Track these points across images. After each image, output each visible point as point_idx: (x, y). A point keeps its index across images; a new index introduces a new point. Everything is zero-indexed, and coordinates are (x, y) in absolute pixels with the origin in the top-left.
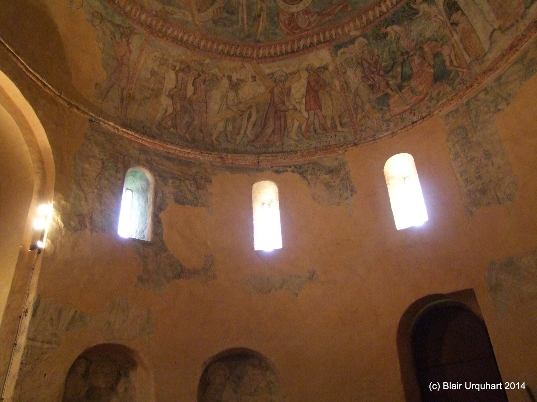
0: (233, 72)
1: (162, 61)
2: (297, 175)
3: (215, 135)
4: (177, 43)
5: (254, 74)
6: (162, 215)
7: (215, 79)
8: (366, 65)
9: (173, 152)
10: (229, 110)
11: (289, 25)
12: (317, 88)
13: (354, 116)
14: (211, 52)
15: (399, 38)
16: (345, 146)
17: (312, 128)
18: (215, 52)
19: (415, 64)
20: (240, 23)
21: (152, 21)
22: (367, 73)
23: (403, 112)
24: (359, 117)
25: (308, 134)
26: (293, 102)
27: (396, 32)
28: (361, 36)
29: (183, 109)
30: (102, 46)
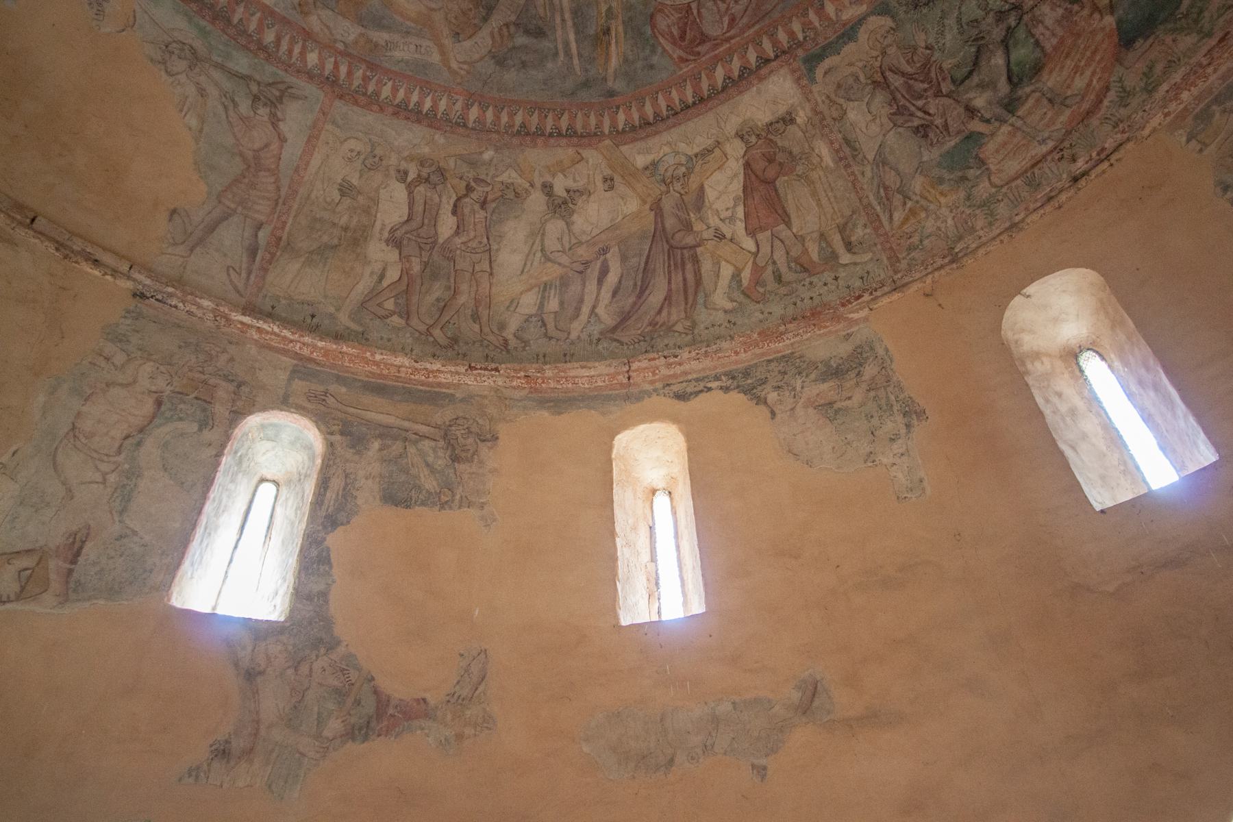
0: (554, 176)
1: (369, 161)
2: (737, 397)
3: (513, 325)
4: (407, 118)
5: (608, 172)
6: (335, 540)
7: (511, 195)
8: (896, 81)
9: (393, 370)
10: (549, 264)
11: (682, 38)
12: (771, 173)
13: (884, 219)
14: (498, 132)
16: (866, 297)
17: (768, 274)
18: (506, 132)
22: (903, 102)
23: (1033, 166)
24: (898, 216)
25: (762, 290)
26: (714, 221)
28: (872, 13)
29: (428, 270)
30: (194, 123)
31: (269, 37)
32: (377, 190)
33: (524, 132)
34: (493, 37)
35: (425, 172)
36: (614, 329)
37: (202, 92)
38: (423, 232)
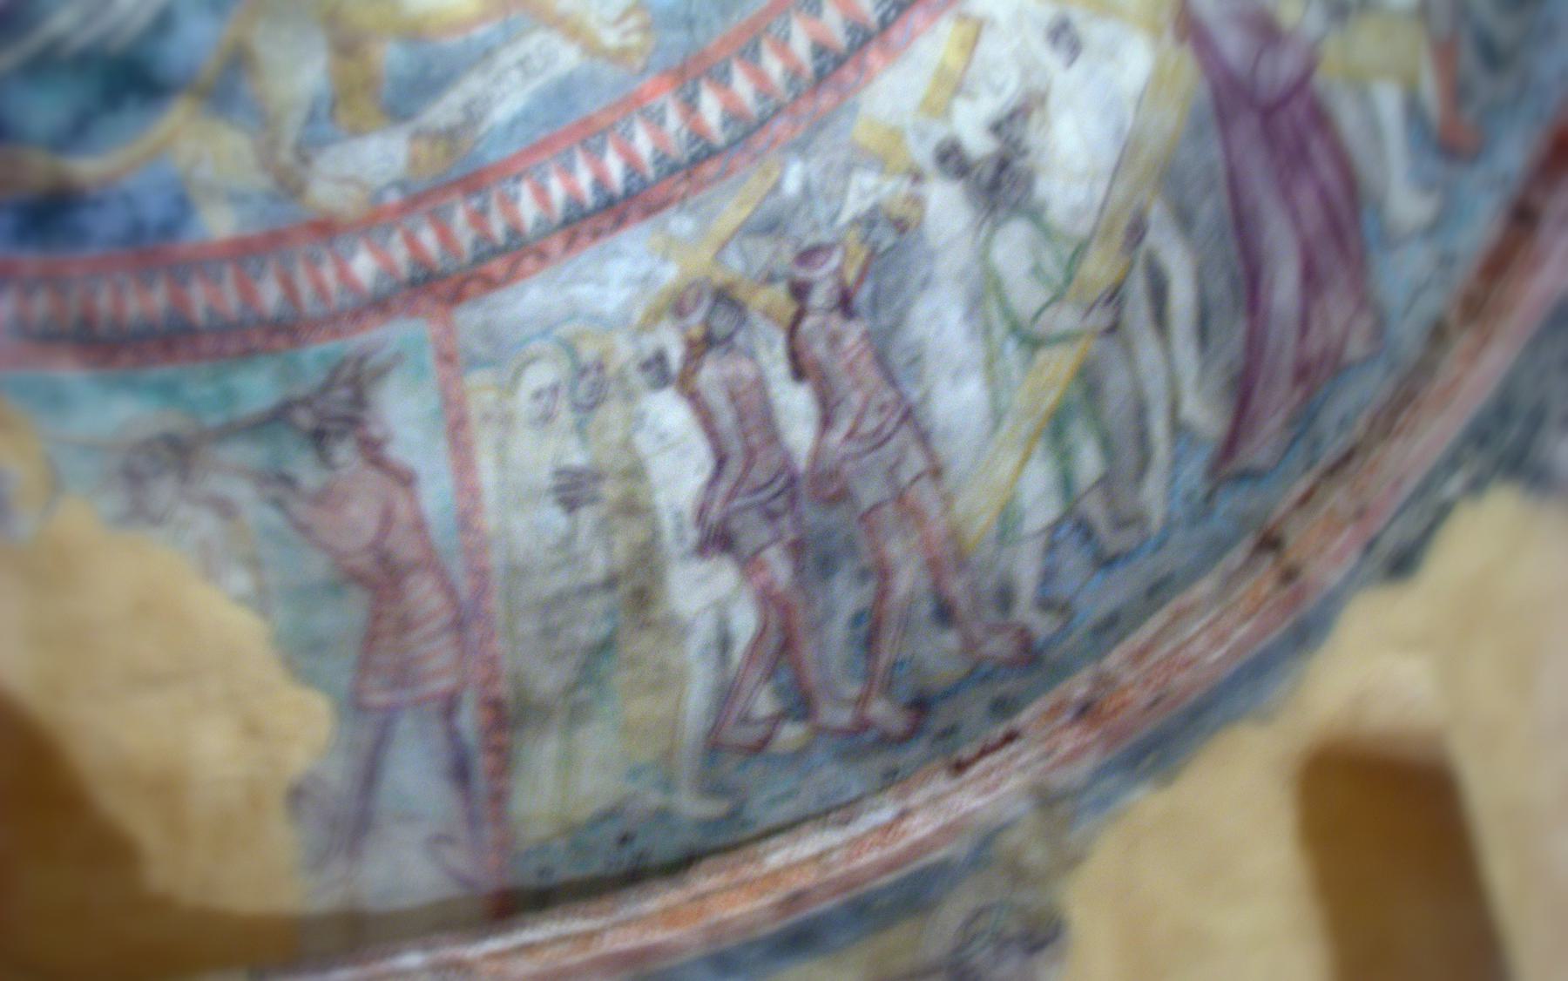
4: (596, 235)
7: (888, 239)
10: (1042, 356)
21: (411, 241)
31: (270, 295)
32: (627, 445)
35: (695, 321)
36: (1231, 445)
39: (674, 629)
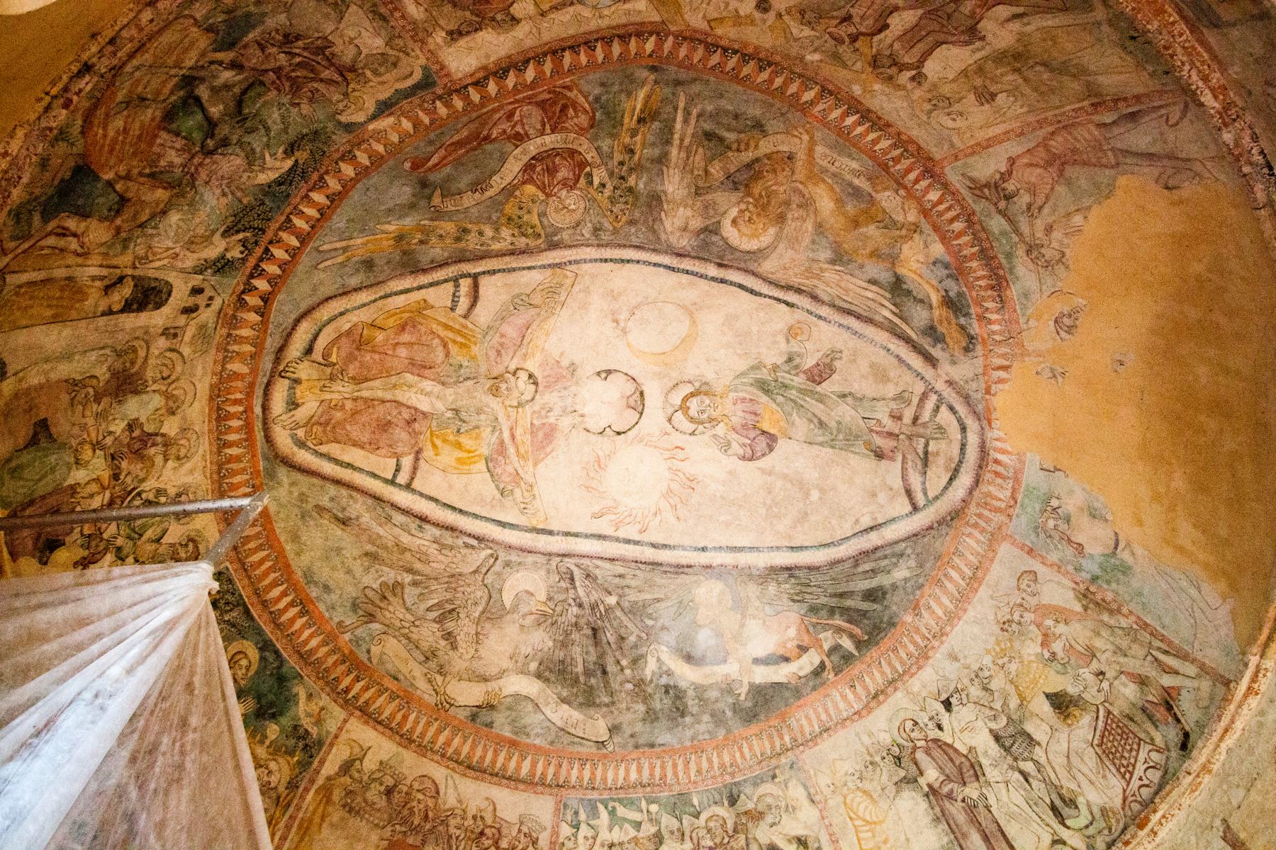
11: (564, 108)
15: (250, 164)
19: (172, 148)
20: (695, 112)
21: (917, 181)
22: (319, 58)
27: (263, 169)
28: (362, 124)
31: (958, 226)
32: (953, 81)
33: (764, 63)
34: (756, 146)
37: (1049, 229)
38: (937, 27)
39: (1021, 37)
